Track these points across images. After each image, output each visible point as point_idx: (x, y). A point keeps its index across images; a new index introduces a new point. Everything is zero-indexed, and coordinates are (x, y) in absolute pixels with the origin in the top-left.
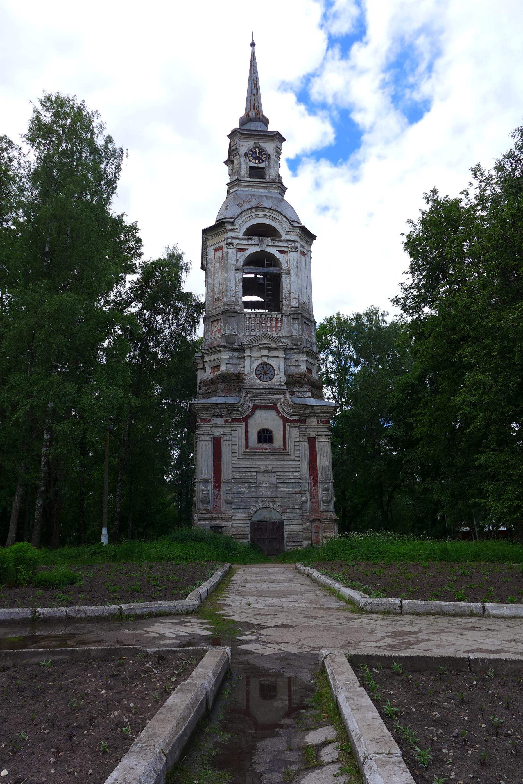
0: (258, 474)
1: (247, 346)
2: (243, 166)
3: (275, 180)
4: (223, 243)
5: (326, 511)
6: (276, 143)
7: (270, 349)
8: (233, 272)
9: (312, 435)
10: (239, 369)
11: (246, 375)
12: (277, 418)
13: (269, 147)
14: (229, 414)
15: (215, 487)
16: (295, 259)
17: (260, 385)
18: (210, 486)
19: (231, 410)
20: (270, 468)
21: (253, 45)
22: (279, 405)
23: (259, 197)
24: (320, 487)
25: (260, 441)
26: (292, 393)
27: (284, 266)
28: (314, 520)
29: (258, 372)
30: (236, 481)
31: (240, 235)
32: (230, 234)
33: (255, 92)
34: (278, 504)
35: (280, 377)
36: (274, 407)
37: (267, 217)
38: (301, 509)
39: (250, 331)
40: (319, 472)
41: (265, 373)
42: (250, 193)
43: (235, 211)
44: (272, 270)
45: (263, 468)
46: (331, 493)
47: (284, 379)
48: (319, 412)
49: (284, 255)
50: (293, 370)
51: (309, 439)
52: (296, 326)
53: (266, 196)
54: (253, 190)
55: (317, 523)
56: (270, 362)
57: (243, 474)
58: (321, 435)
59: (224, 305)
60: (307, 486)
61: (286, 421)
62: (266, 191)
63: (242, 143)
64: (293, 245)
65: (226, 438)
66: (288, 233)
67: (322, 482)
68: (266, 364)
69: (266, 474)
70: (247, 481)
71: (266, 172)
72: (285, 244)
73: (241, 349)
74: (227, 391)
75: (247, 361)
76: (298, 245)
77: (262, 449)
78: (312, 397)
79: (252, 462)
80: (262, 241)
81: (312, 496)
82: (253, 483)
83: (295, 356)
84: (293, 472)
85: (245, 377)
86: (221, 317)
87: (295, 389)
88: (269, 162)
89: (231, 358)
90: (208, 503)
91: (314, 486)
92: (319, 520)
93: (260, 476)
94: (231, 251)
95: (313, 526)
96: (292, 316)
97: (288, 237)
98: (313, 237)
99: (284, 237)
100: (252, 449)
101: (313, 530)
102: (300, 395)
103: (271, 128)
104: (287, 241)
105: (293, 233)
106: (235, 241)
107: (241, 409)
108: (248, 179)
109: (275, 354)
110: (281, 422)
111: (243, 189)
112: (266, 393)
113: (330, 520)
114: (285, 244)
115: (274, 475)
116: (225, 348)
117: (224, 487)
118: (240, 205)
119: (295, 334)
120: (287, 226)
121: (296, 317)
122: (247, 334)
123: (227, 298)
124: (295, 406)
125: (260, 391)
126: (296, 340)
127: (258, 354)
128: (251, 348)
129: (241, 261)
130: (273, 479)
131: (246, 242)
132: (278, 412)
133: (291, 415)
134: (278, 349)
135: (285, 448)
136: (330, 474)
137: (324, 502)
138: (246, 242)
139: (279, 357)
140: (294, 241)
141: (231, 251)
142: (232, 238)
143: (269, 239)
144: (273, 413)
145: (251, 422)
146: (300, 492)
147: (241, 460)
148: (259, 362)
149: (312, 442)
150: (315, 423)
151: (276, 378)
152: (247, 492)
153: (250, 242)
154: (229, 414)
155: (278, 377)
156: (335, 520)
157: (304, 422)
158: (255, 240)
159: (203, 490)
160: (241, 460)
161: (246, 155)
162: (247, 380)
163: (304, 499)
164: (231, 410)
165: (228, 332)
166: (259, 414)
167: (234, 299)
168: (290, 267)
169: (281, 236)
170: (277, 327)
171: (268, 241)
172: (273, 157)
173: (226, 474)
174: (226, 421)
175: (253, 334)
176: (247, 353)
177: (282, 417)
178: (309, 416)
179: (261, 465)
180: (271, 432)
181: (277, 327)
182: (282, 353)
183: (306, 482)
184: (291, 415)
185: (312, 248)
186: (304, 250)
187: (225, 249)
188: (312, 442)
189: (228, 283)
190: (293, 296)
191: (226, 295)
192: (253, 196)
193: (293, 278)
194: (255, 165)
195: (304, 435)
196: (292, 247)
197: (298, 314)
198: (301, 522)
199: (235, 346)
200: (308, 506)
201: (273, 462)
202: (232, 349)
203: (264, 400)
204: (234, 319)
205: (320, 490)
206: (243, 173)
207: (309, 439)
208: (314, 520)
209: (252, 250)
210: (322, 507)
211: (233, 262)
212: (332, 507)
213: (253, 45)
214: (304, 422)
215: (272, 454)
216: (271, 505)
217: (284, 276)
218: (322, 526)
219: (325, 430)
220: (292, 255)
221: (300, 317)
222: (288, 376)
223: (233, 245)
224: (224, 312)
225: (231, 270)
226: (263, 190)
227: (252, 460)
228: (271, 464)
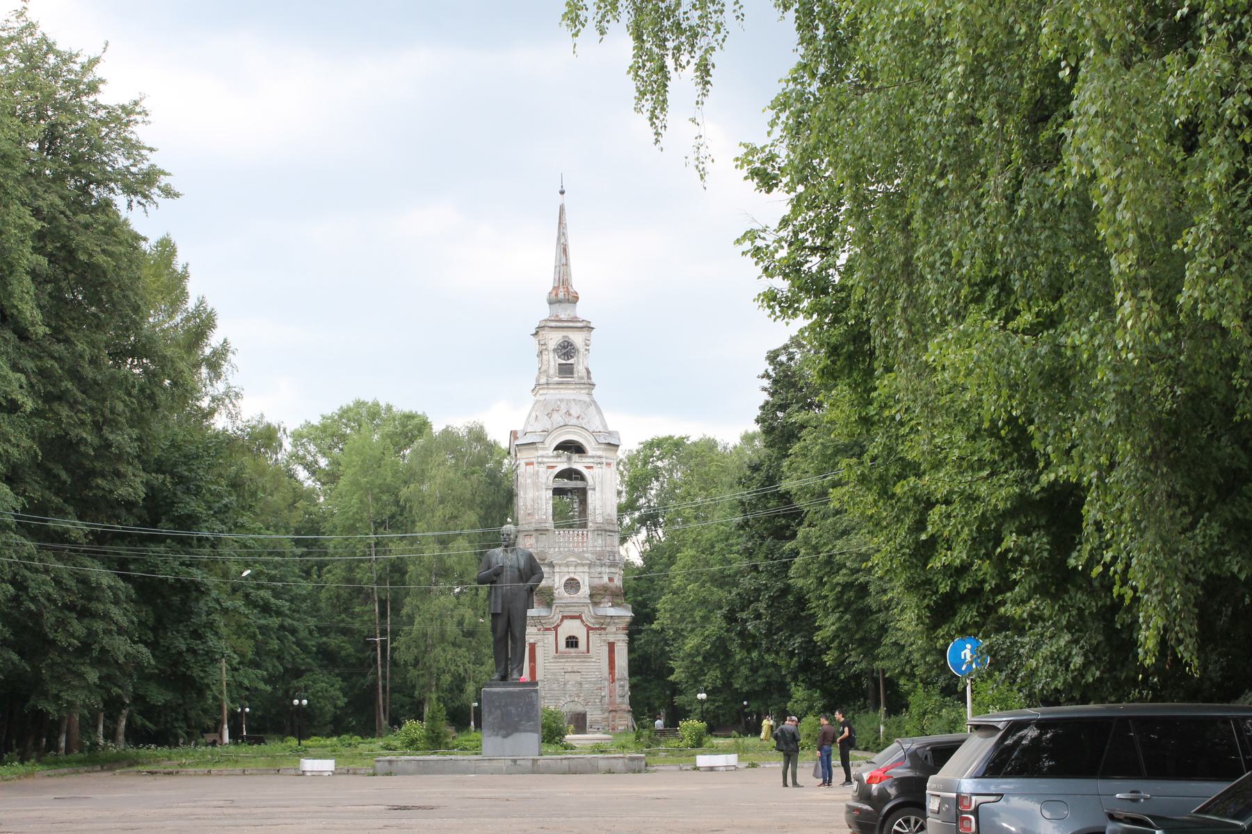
2: (552, 363)
3: (582, 378)
4: (533, 460)
7: (576, 566)
9: (612, 640)
13: (577, 338)
23: (568, 401)
24: (617, 684)
25: (567, 646)
26: (595, 604)
27: (590, 481)
31: (550, 452)
32: (540, 453)
33: (564, 261)
35: (585, 590)
36: (579, 617)
37: (575, 433)
43: (546, 423)
44: (579, 484)
46: (627, 688)
50: (597, 582)
53: (574, 400)
54: (562, 391)
55: (614, 714)
56: (576, 577)
57: (554, 674)
60: (607, 683)
61: (589, 629)
63: (551, 336)
64: (599, 460)
65: (539, 644)
66: (594, 449)
68: (573, 579)
75: (557, 579)
76: (604, 460)
78: (612, 606)
80: (569, 459)
81: (611, 691)
83: (599, 570)
86: (534, 533)
93: (567, 676)
94: (542, 469)
99: (590, 452)
104: (593, 457)
105: (599, 449)
106: (545, 460)
108: (557, 379)
109: (580, 569)
110: (585, 629)
111: (552, 391)
114: (592, 460)
118: (549, 415)
124: (597, 617)
127: (565, 569)
128: (560, 565)
129: (551, 478)
130: (578, 677)
131: (555, 460)
132: (582, 621)
134: (583, 565)
135: (588, 651)
136: (626, 674)
140: (600, 457)
141: (542, 469)
142: (542, 456)
143: (577, 455)
144: (579, 621)
145: (560, 629)
148: (567, 577)
149: (611, 646)
150: (614, 630)
153: (559, 460)
154: (541, 624)
157: (605, 629)
158: (564, 458)
170: (583, 543)
171: (575, 457)
172: (582, 350)
174: (539, 630)
176: (557, 569)
177: (586, 625)
178: (609, 624)
179: (569, 666)
181: (583, 543)
182: (586, 569)
186: (610, 461)
187: (535, 465)
188: (611, 646)
190: (597, 512)
192: (561, 400)
194: (564, 362)
198: (600, 712)
199: (546, 561)
200: (606, 700)
205: (617, 686)
206: (552, 371)
208: (612, 711)
209: (563, 466)
210: (618, 700)
211: (544, 480)
212: (627, 700)
214: (605, 629)
215: (577, 657)
217: (590, 493)
218: (618, 715)
220: (597, 470)
222: (592, 588)
224: (537, 530)
228: (577, 666)
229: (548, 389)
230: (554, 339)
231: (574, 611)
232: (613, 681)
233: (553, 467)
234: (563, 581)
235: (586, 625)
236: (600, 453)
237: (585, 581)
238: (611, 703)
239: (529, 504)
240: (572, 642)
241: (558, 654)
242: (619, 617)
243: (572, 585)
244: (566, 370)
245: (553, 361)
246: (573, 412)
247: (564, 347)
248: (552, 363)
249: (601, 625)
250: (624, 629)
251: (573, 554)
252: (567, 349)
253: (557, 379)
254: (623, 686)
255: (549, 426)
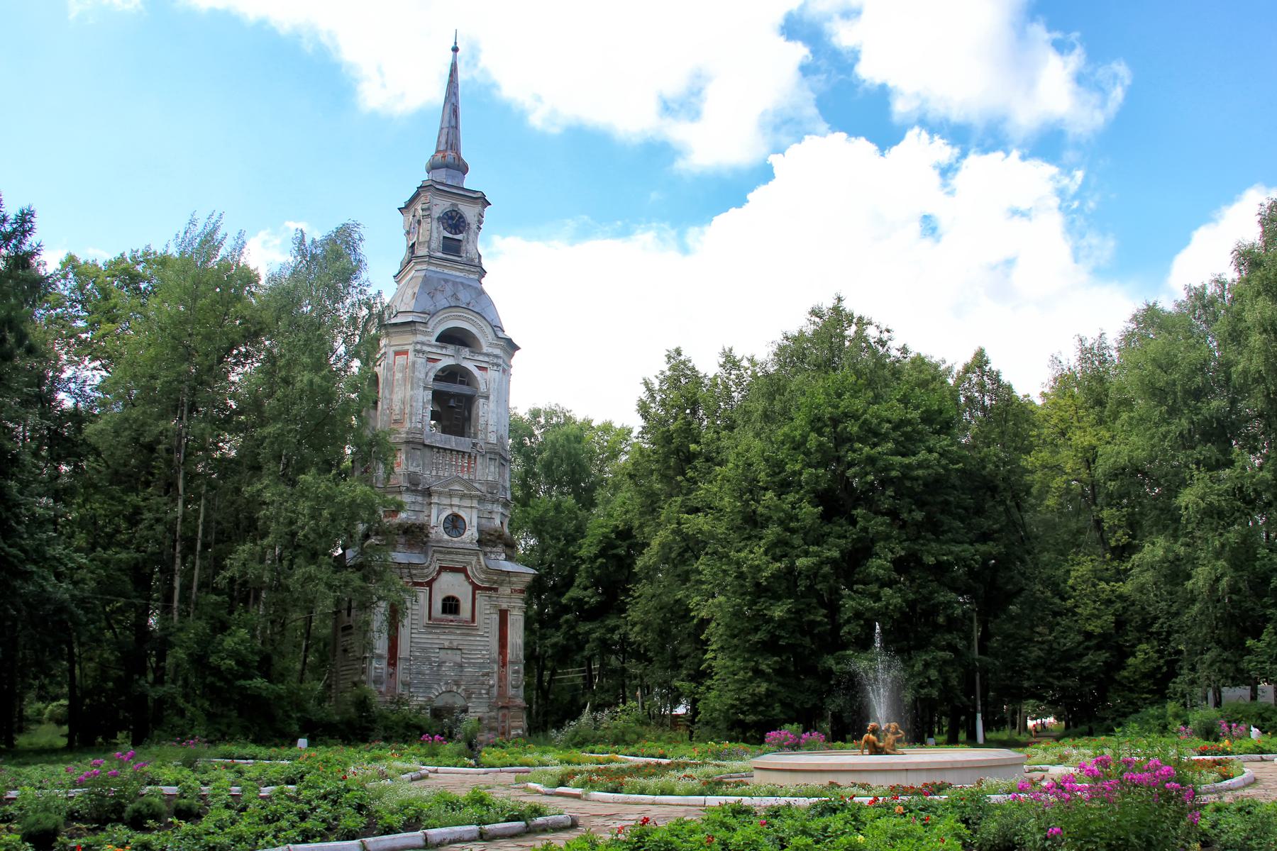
0: (442, 651)
1: (436, 492)
2: (435, 235)
3: (473, 260)
4: (410, 348)
5: (516, 696)
6: (477, 209)
7: (463, 497)
8: (421, 389)
9: (504, 606)
10: (422, 518)
11: (433, 528)
12: (466, 583)
13: (469, 211)
14: (411, 576)
15: (389, 664)
16: (497, 380)
17: (448, 541)
18: (384, 664)
19: (414, 572)
20: (455, 644)
21: (455, 50)
22: (469, 568)
23: (455, 284)
25: (444, 611)
27: (482, 388)
28: (502, 707)
29: (447, 525)
30: (416, 658)
31: (433, 340)
32: (420, 338)
33: (453, 123)
34: (463, 687)
35: (471, 533)
36: (463, 570)
37: (467, 320)
38: (488, 694)
39: (437, 469)
40: (509, 651)
41: (455, 527)
42: (442, 276)
44: (464, 389)
45: (447, 644)
47: (476, 536)
48: (514, 579)
49: (484, 373)
51: (500, 611)
52: (492, 468)
54: (446, 271)
55: (505, 711)
56: (462, 513)
57: (424, 650)
58: (514, 607)
59: (407, 433)
60: (496, 667)
61: (476, 588)
62: (462, 275)
63: (436, 201)
66: (491, 345)
67: (512, 663)
69: (449, 652)
70: (428, 658)
71: (463, 248)
72: (486, 359)
73: (428, 493)
74: (410, 546)
77: (447, 621)
79: (435, 636)
80: (458, 351)
81: (500, 679)
82: (435, 662)
83: (489, 507)
84: (481, 650)
85: (432, 531)
87: (488, 549)
88: (468, 234)
89: (413, 502)
90: (382, 684)
91: (503, 667)
92: (507, 708)
93: (442, 654)
95: (500, 714)
96: (488, 456)
97: (490, 350)
98: (516, 348)
99: (485, 349)
100: (436, 620)
101: (500, 719)
102: (493, 556)
103: (469, 182)
104: (488, 355)
107: (426, 571)
108: (440, 255)
109: (467, 503)
110: (470, 588)
112: (457, 554)
113: (518, 707)
114: (486, 359)
115: (459, 652)
116: (408, 489)
117: (401, 666)
118: (432, 295)
119: (490, 478)
120: (491, 336)
121: (493, 456)
122: (434, 473)
123: (411, 422)
124: (487, 571)
125: (450, 551)
126: (492, 486)
127: (446, 501)
128: (440, 494)
129: (432, 375)
131: (439, 351)
132: (467, 576)
133: (483, 581)
134: (471, 497)
137: (513, 687)
138: (439, 351)
139: (471, 507)
140: (497, 356)
141: (421, 360)
142: (423, 344)
143: (467, 349)
144: (461, 577)
145: (435, 586)
146: (487, 674)
147: (422, 633)
148: (448, 512)
149: (503, 615)
151: (467, 533)
152: (428, 672)
153: (444, 352)
154: (411, 576)
155: (470, 533)
156: (525, 708)
157: (496, 590)
158: (450, 349)
159: (376, 668)
160: (422, 633)
161: (439, 219)
162: (433, 534)
163: (491, 682)
164: (414, 572)
165: (412, 469)
166: (446, 578)
167: (420, 426)
168: (488, 390)
169: (481, 347)
170: (469, 467)
171: (466, 352)
172: (474, 227)
173: (403, 650)
175: (441, 473)
176: (435, 499)
177: (472, 583)
178: (501, 584)
179: (445, 640)
180: (458, 601)
182: (475, 504)
183: (493, 661)
184: (483, 581)
185: (514, 361)
187: (411, 356)
188: (503, 615)
189: (414, 404)
190: (490, 428)
191: (411, 420)
192: (446, 281)
193: (492, 405)
194: (450, 236)
195: (495, 606)
196: (494, 364)
197: (496, 454)
198: (488, 710)
200: (495, 691)
201: (460, 637)
202: (415, 492)
203: (452, 561)
204: (419, 452)
206: (434, 245)
207: (500, 611)
208: (502, 707)
210: (511, 692)
211: (422, 376)
212: (521, 692)
213: (455, 50)
214: (496, 590)
215: (458, 627)
216: (455, 688)
219: (519, 601)
220: (492, 374)
221: (497, 457)
222: (480, 531)
223: (424, 352)
224: (407, 442)
225: (419, 386)
226: (458, 274)
227: (435, 633)
228: (456, 639)
229: (429, 263)
230: (442, 206)
231: (458, 561)
232: (504, 665)
233: (435, 360)
234: (443, 517)
235: (472, 583)
236: (497, 351)
237: (471, 518)
238: (502, 695)
239: (397, 407)
240: (451, 605)
241: (433, 625)
242: (517, 574)
243: (455, 524)
244: (452, 247)
245: (434, 233)
246: (461, 296)
247: (452, 218)
248: (435, 235)
249: (489, 586)
250: (522, 591)
251: (459, 480)
252: (455, 222)
253: (440, 255)
254: (517, 672)
255: (432, 309)
